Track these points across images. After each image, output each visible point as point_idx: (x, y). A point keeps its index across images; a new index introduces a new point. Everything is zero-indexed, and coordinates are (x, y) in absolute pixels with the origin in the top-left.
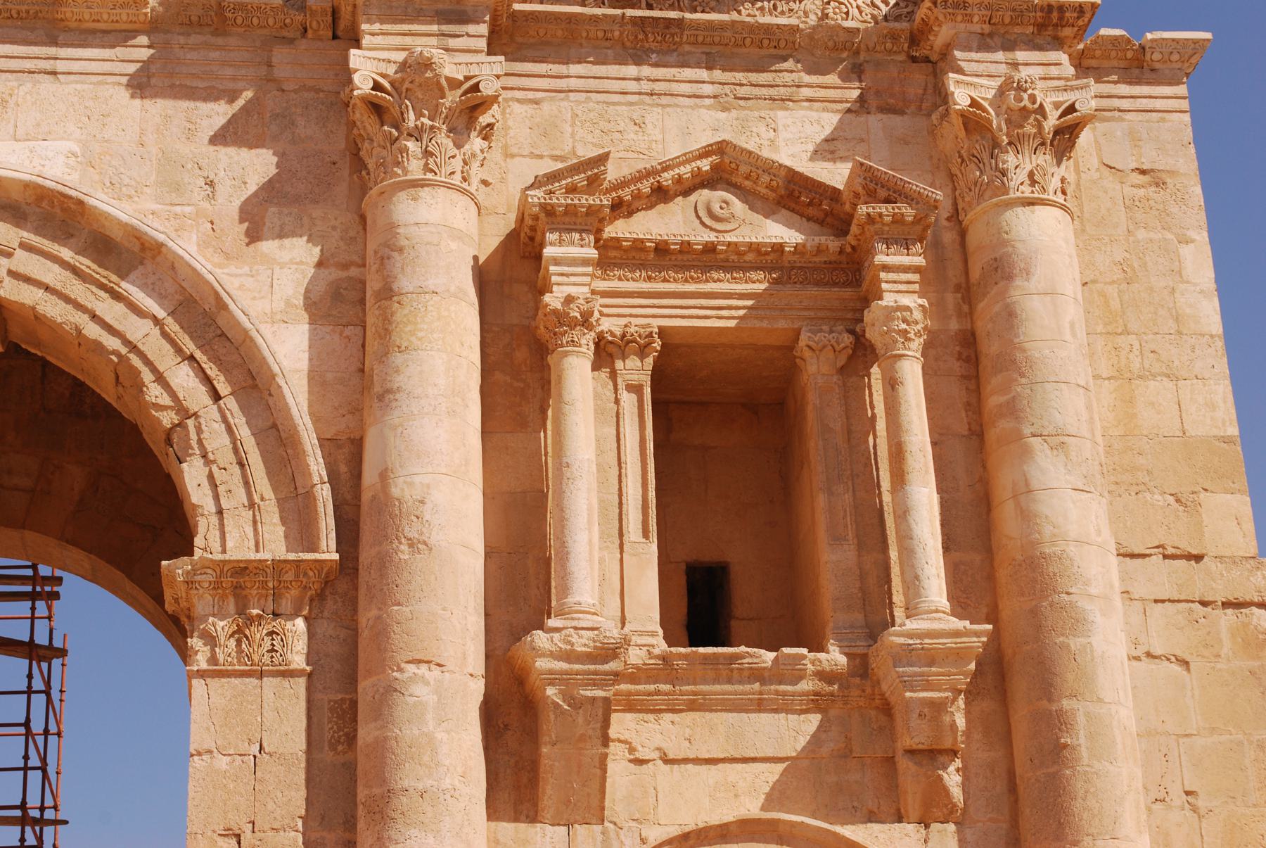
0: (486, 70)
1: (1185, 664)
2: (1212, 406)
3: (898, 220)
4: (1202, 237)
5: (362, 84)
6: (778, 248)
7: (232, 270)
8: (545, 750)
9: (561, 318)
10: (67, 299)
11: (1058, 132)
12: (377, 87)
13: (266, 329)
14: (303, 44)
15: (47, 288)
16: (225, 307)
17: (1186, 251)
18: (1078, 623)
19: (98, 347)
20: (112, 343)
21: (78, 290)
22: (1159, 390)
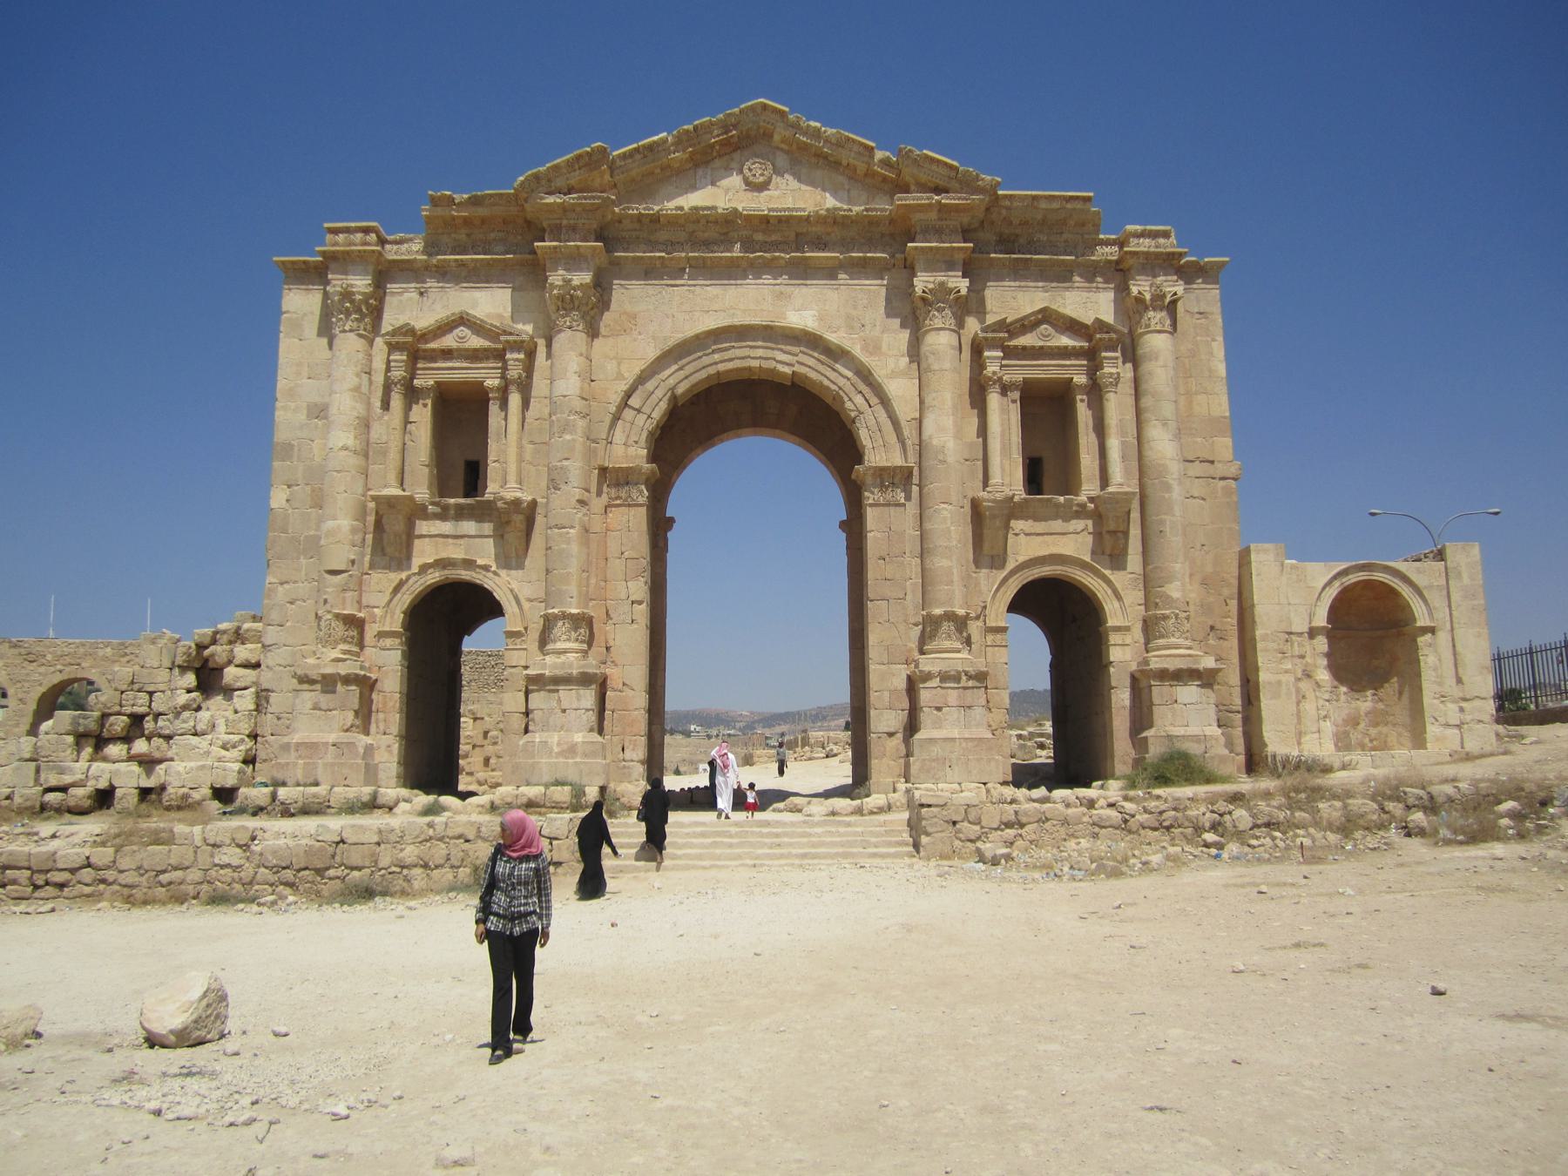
0: (962, 284)
1: (1203, 499)
2: (1220, 405)
3: (1110, 339)
4: (1220, 339)
5: (918, 290)
6: (1066, 347)
7: (872, 358)
8: (985, 531)
9: (990, 379)
10: (816, 371)
11: (1170, 302)
12: (924, 292)
13: (886, 381)
14: (894, 270)
15: (810, 367)
16: (872, 374)
17: (1214, 344)
18: (1168, 488)
19: (828, 388)
20: (833, 387)
21: (821, 368)
22: (1201, 398)
